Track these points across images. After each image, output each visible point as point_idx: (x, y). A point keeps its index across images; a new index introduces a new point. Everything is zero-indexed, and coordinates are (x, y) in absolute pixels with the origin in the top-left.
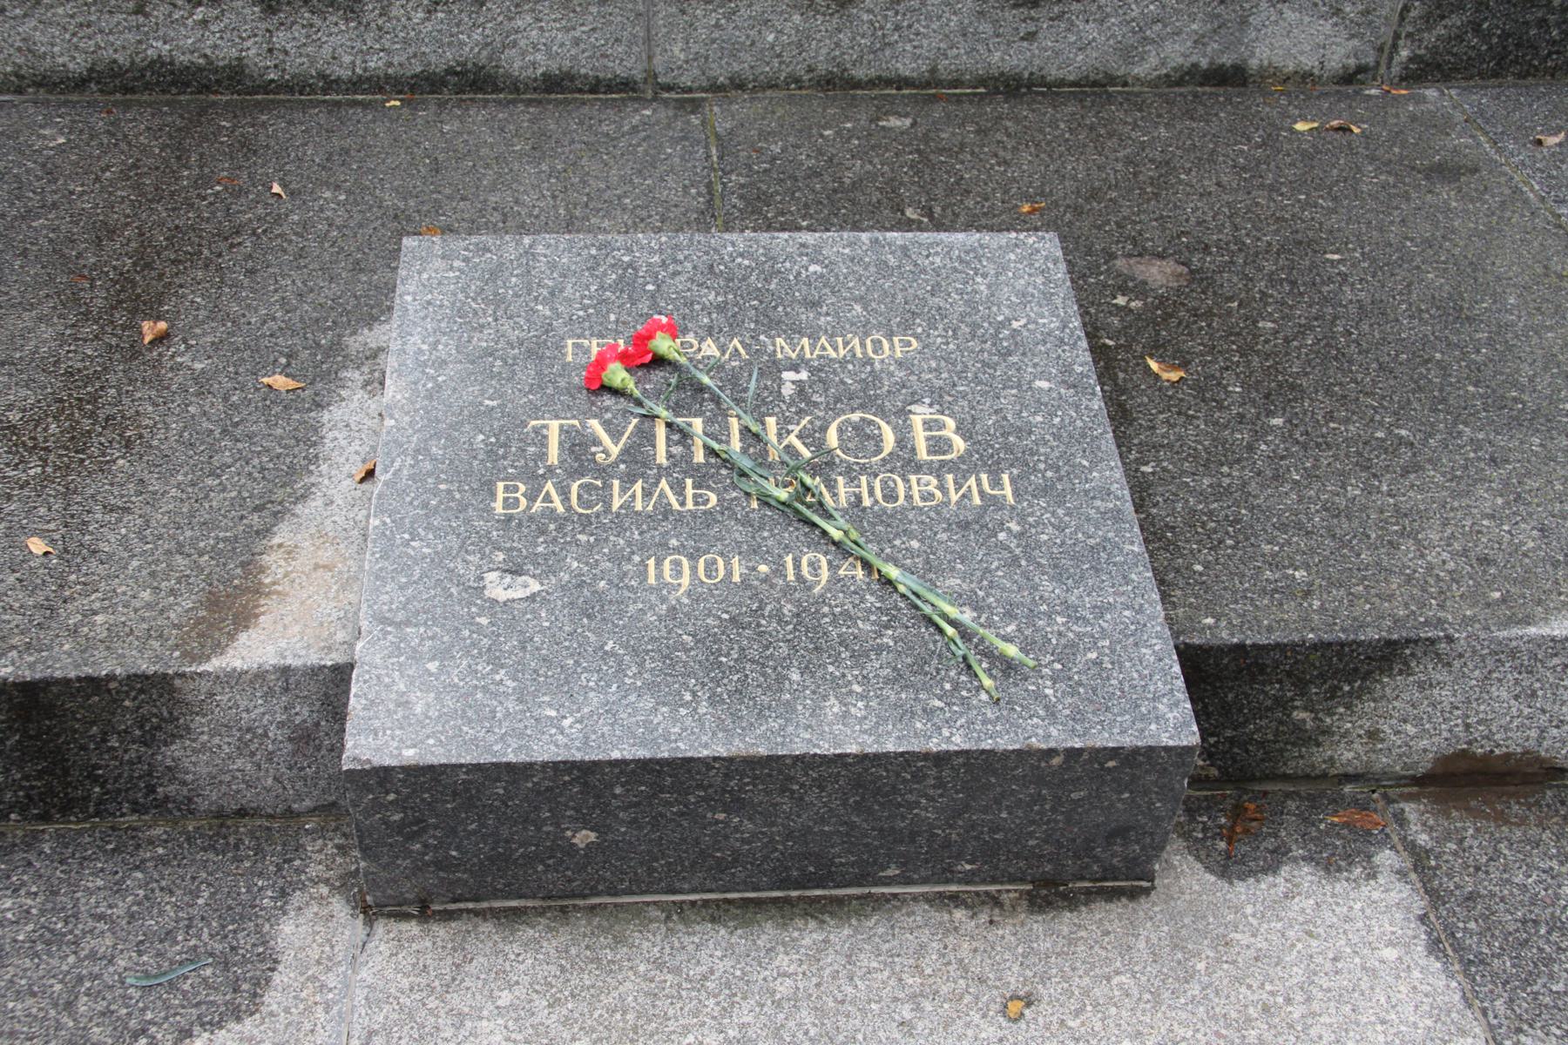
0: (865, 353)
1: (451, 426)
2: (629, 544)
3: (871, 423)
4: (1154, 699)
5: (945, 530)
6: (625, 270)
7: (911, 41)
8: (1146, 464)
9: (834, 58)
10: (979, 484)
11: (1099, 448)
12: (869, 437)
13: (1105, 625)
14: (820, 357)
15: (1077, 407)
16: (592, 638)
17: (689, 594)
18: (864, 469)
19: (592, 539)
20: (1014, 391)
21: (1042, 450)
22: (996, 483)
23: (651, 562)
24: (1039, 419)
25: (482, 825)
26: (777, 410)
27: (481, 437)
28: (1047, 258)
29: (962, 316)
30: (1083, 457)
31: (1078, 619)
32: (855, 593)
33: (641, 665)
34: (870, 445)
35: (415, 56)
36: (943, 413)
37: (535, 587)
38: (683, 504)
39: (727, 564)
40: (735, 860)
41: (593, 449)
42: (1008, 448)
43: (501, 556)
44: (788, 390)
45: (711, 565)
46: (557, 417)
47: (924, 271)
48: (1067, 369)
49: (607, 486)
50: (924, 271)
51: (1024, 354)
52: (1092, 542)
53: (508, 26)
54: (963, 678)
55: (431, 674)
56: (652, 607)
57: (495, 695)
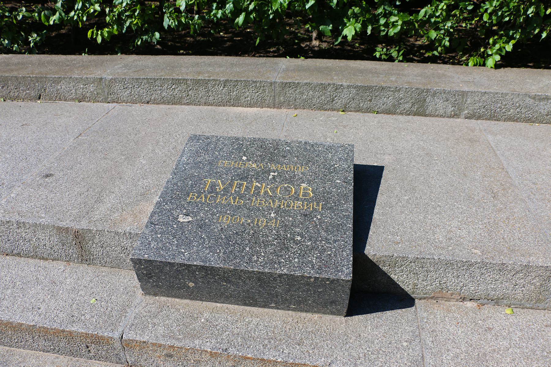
1: (185, 179)
2: (217, 211)
3: (289, 187)
10: (313, 205)
15: (346, 188)
22: (318, 205)
25: (166, 277)
34: (287, 193)
37: (190, 219)
40: (231, 296)
42: (324, 197)
43: (185, 211)
44: (271, 177)
48: (346, 178)
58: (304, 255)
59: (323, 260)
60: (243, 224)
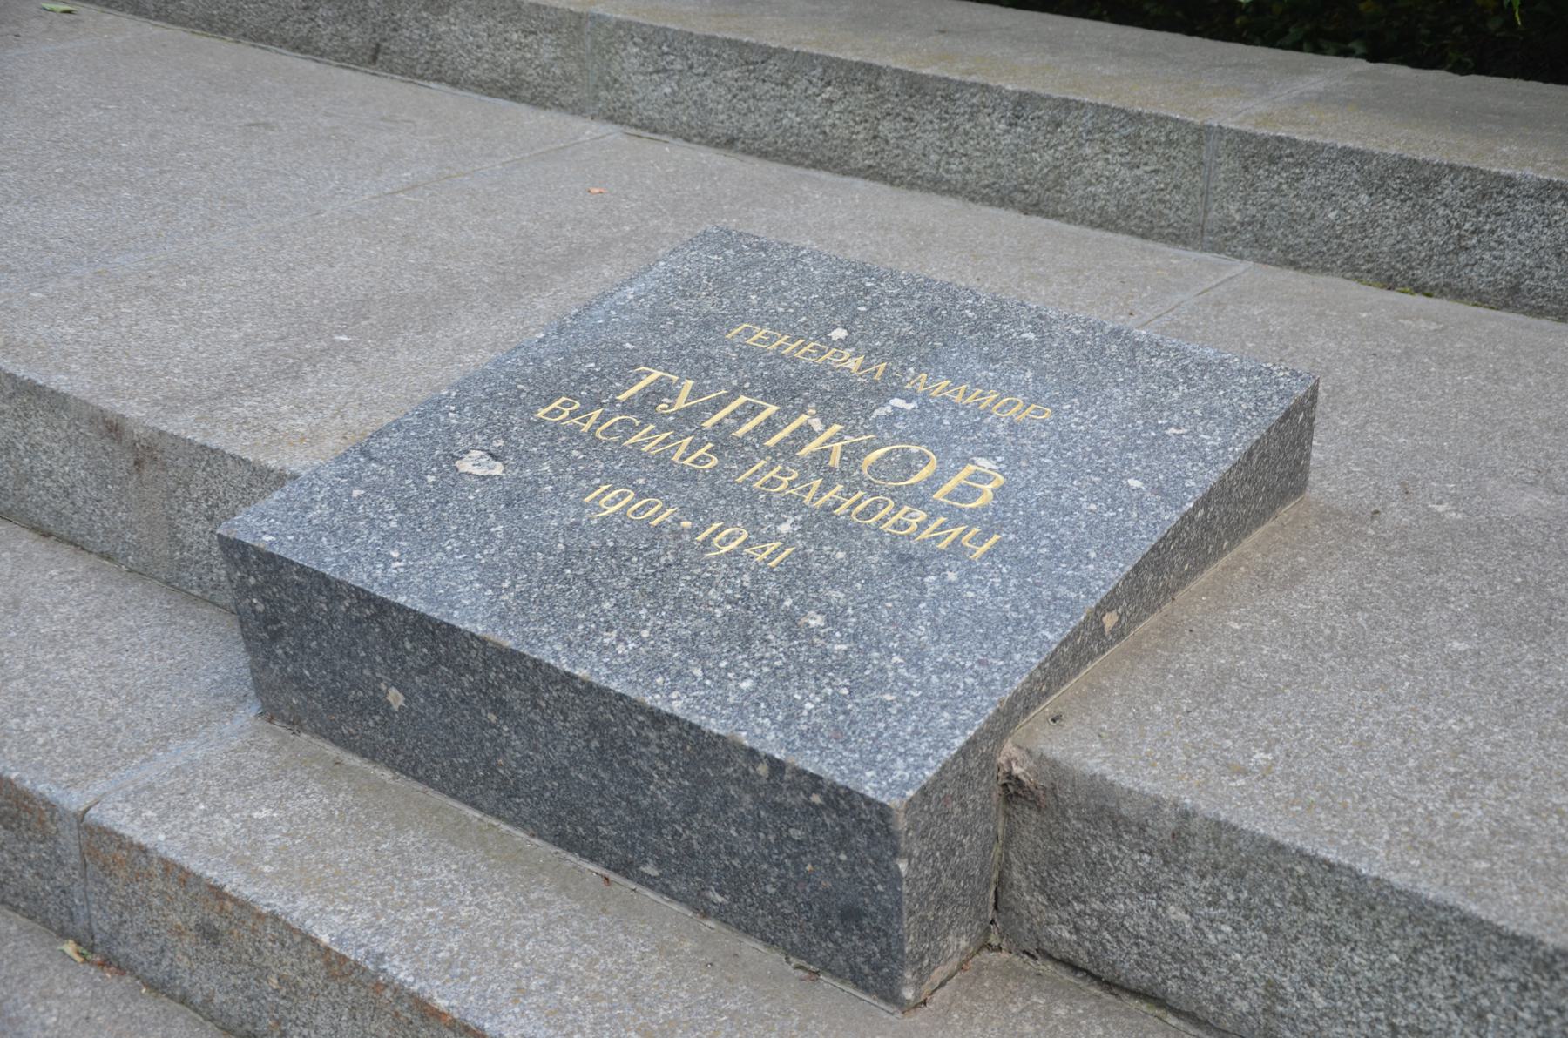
7: (1491, 249)
9: (1399, 252)
35: (991, 166)
43: (501, 443)
53: (1077, 152)
58: (788, 677)
59: (846, 713)
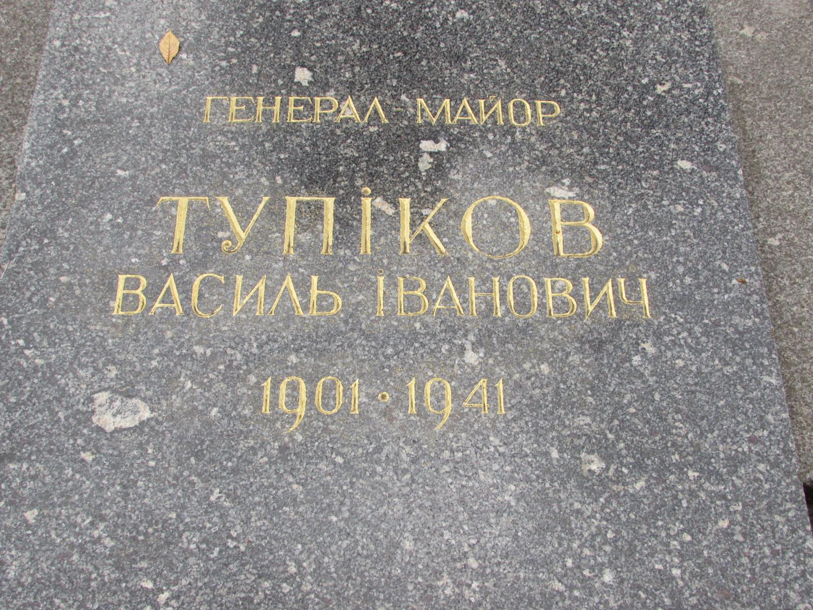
0: (507, 120)
3: (509, 208)
4: (786, 585)
5: (580, 350)
6: (273, 12)
8: (773, 235)
11: (740, 248)
12: (505, 226)
13: (738, 482)
14: (461, 123)
16: (200, 485)
17: (303, 427)
18: (496, 270)
19: (209, 352)
20: (655, 173)
21: (682, 249)
22: (633, 287)
23: (267, 385)
24: (680, 208)
26: (412, 189)
27: (109, 216)
28: (693, 9)
29: (609, 75)
30: (723, 258)
31: (711, 473)
32: (478, 432)
33: (247, 522)
34: (505, 237)
36: (582, 199)
38: (306, 308)
39: (347, 390)
41: (220, 234)
42: (646, 244)
43: (113, 372)
44: (425, 164)
45: (329, 389)
46: (187, 193)
47: (570, 21)
49: (230, 284)
50: (570, 21)
51: (667, 126)
52: (728, 370)
54: (587, 552)
55: (28, 527)
56: (263, 445)
57: (92, 557)
58: (632, 550)
60: (364, 417)
